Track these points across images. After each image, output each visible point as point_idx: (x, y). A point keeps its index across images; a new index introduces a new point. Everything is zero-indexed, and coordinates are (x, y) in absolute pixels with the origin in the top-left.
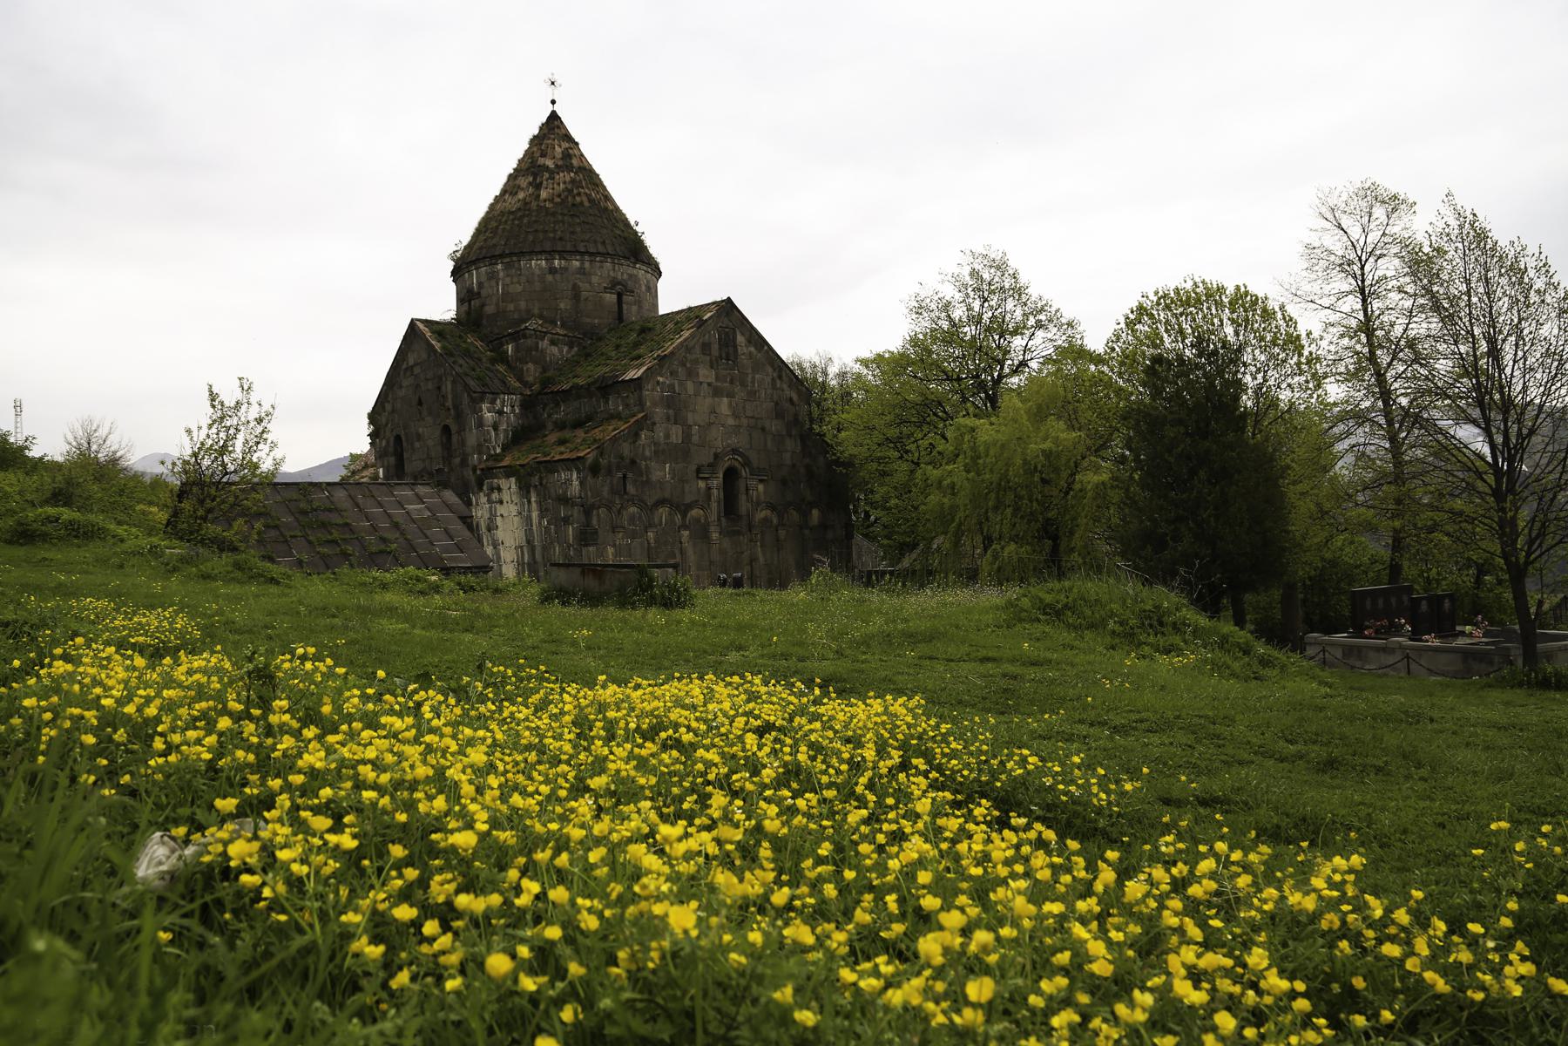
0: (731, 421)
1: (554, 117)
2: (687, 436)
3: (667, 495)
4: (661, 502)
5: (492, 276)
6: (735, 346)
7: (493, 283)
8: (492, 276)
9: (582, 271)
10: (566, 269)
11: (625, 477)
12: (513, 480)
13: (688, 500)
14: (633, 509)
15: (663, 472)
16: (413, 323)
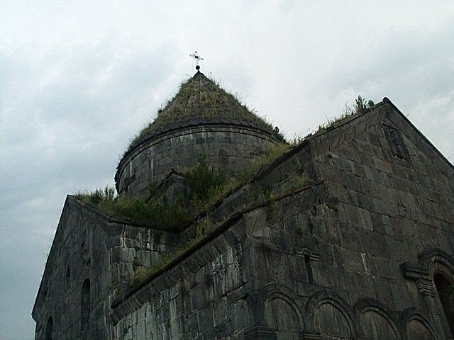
0: (422, 219)
1: (199, 75)
2: (378, 224)
3: (372, 296)
4: (366, 303)
5: (146, 159)
6: (404, 147)
7: (146, 163)
8: (146, 159)
9: (228, 140)
10: (213, 139)
11: (307, 259)
12: (147, 306)
13: (401, 306)
14: (329, 309)
15: (359, 262)
16: (68, 195)
